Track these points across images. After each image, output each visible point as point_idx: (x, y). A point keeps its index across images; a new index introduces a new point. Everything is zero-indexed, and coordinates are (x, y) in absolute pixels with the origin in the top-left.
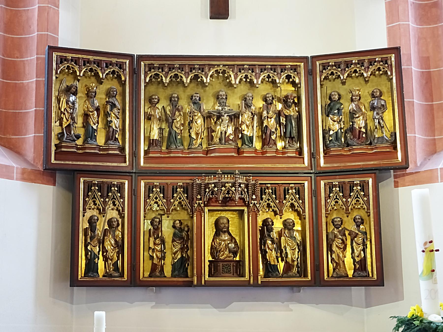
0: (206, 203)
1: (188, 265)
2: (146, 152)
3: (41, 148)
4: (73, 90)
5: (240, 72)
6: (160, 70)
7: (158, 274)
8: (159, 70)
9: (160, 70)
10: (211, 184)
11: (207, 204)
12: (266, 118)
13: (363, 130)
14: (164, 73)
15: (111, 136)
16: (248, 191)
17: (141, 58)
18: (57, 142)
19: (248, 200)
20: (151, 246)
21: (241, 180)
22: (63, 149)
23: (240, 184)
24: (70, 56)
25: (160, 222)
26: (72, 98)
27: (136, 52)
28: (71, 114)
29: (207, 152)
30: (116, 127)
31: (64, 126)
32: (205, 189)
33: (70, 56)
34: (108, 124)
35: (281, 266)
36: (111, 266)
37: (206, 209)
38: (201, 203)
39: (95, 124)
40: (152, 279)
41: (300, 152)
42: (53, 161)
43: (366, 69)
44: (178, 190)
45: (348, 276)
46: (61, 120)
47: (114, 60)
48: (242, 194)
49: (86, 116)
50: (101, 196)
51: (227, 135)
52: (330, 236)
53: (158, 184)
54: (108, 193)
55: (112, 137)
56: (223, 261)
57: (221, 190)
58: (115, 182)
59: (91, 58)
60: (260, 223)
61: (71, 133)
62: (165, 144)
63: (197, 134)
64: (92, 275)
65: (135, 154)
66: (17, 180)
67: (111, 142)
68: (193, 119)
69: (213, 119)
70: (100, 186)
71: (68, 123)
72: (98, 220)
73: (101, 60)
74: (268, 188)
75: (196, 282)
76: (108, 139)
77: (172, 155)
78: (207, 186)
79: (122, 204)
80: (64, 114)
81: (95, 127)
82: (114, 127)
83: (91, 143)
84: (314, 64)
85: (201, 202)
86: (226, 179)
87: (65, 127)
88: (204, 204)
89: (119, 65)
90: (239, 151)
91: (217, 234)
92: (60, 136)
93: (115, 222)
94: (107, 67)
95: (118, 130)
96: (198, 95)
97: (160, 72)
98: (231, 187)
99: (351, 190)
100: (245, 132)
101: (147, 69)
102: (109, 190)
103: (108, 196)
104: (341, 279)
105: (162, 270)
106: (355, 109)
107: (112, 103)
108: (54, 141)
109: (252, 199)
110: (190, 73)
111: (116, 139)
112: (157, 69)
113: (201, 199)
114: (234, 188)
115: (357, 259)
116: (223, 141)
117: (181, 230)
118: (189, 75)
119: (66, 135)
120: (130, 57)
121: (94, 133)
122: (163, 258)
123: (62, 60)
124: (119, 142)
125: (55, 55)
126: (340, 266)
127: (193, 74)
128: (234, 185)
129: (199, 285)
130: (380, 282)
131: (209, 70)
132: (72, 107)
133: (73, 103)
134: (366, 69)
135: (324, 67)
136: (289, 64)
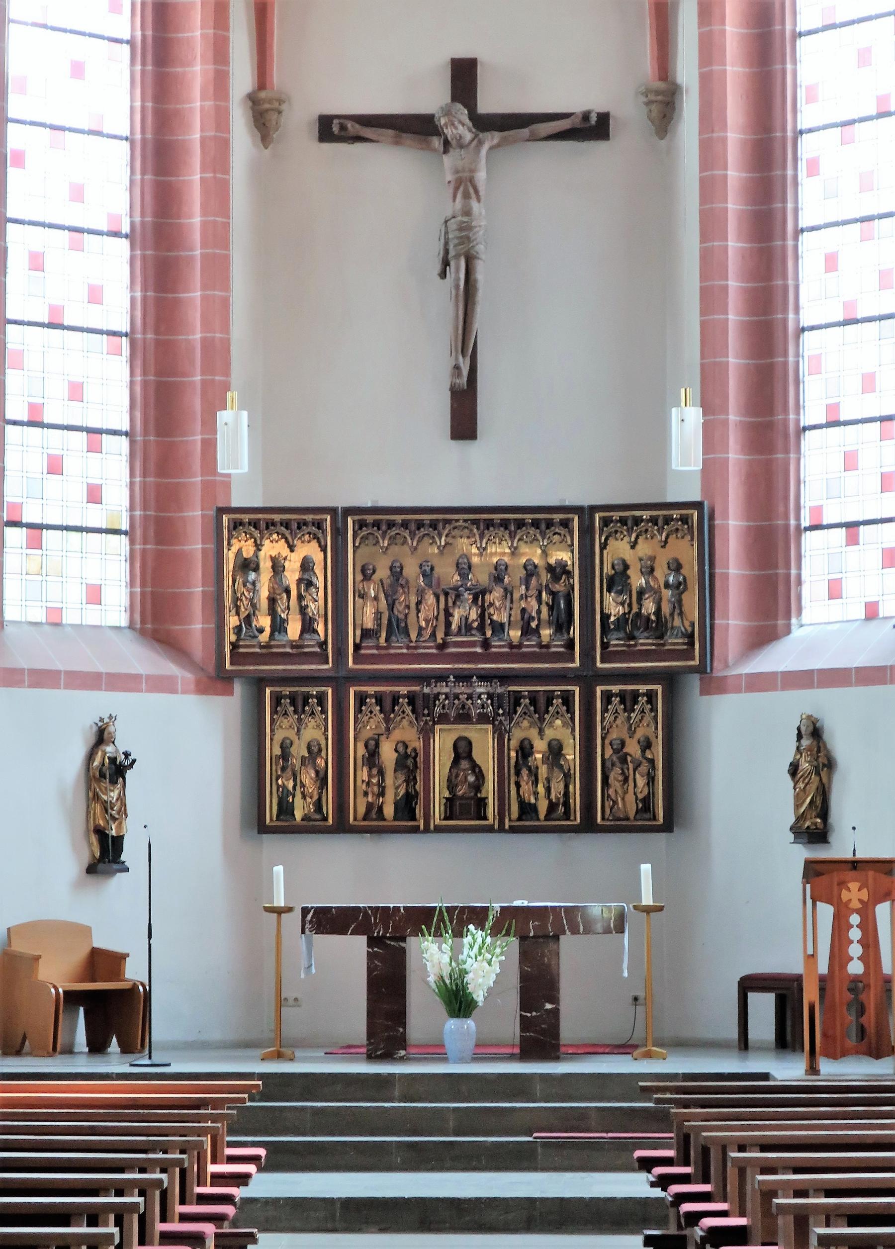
0: (436, 719)
1: (416, 803)
2: (357, 647)
3: (213, 645)
4: (253, 566)
5: (488, 529)
6: (375, 528)
7: (374, 816)
8: (373, 528)
9: (375, 528)
10: (442, 694)
11: (438, 721)
12: (524, 596)
13: (653, 617)
14: (380, 532)
15: (308, 626)
16: (492, 704)
17: (349, 511)
18: (233, 638)
19: (493, 715)
20: (364, 779)
21: (481, 689)
22: (241, 650)
23: (481, 694)
24: (246, 518)
25: (377, 745)
26: (252, 576)
27: (342, 501)
28: (251, 600)
29: (443, 646)
30: (313, 613)
31: (242, 616)
32: (435, 702)
33: (246, 518)
34: (303, 610)
35: (543, 807)
36: (311, 806)
37: (437, 727)
38: (430, 721)
39: (284, 612)
40: (366, 823)
41: (570, 645)
42: (228, 666)
43: (661, 529)
44: (401, 700)
45: (627, 819)
46: (238, 608)
47: (309, 517)
48: (483, 707)
49: (272, 601)
50: (295, 712)
51: (470, 620)
52: (609, 764)
53: (373, 692)
54: (304, 707)
55: (309, 627)
56: (462, 798)
57: (454, 704)
58: (314, 691)
59: (277, 517)
60: (514, 743)
61: (250, 625)
62: (384, 635)
63: (427, 621)
64: (285, 818)
65: (340, 653)
66: (183, 693)
67: (307, 636)
68: (421, 598)
69: (451, 598)
70: (293, 699)
71: (247, 613)
72: (291, 744)
73: (290, 520)
74: (524, 697)
75: (422, 827)
76: (303, 632)
77: (392, 651)
78: (437, 696)
79: (324, 721)
80: (241, 600)
81: (283, 616)
82: (310, 614)
83: (280, 638)
84: (592, 519)
85: (428, 718)
86: (462, 689)
87: (244, 619)
88: (434, 721)
89: (316, 525)
90: (486, 644)
91: (456, 762)
92: (238, 630)
93: (315, 746)
94: (299, 528)
95: (317, 618)
96: (429, 564)
97: (375, 531)
98: (467, 699)
99: (635, 702)
100: (495, 618)
101: (357, 527)
102: (306, 702)
103: (304, 711)
104: (619, 823)
105: (380, 809)
106: (644, 585)
107: (307, 580)
108: (229, 636)
109: (499, 715)
110: (417, 532)
111: (315, 631)
112: (370, 527)
113: (428, 715)
114: (470, 702)
115: (640, 796)
116: (463, 631)
117: (406, 756)
118: (415, 534)
119: (244, 629)
120: (332, 511)
121: (284, 623)
122: (382, 794)
123: (236, 525)
124: (318, 634)
125: (225, 518)
126: (618, 805)
127: (422, 533)
128: (470, 697)
129: (427, 830)
130: (668, 827)
131: (444, 528)
132: (252, 589)
133: (254, 584)
134: (661, 529)
135: (606, 522)
136: (557, 517)
